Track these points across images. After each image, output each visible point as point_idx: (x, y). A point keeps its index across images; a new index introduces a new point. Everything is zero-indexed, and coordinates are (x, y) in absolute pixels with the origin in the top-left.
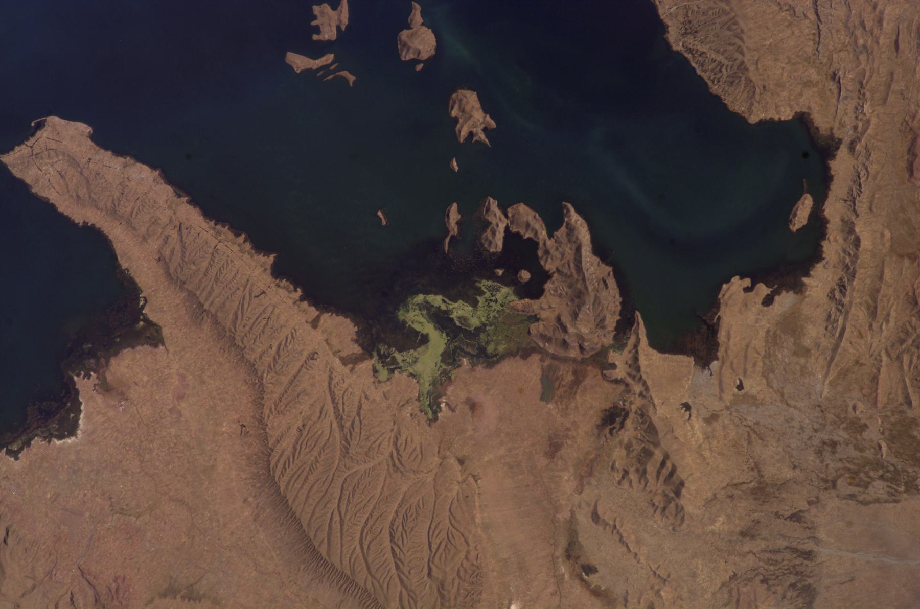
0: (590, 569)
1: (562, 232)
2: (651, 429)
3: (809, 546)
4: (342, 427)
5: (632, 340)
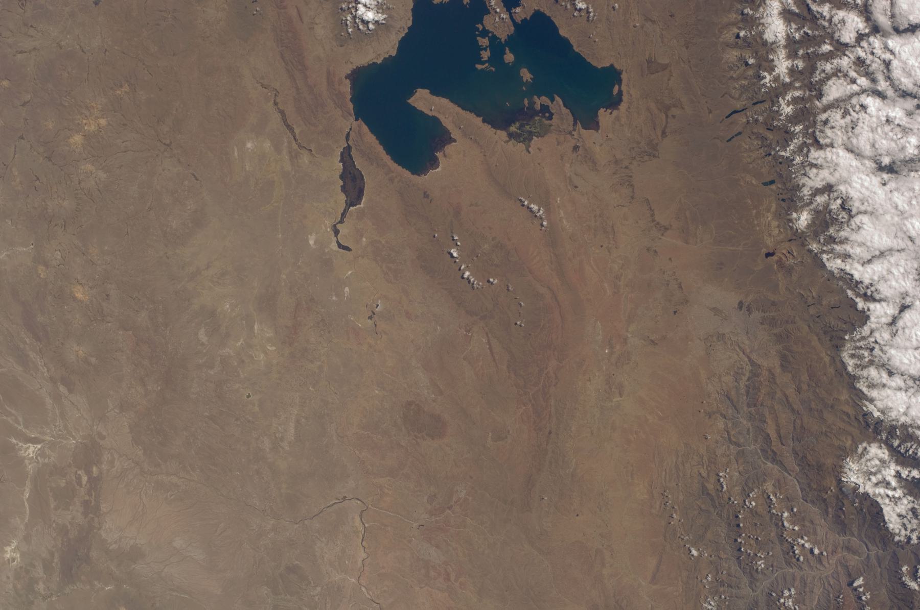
0: (576, 187)
1: (555, 102)
2: (586, 150)
3: (631, 174)
4: (507, 159)
5: (577, 128)
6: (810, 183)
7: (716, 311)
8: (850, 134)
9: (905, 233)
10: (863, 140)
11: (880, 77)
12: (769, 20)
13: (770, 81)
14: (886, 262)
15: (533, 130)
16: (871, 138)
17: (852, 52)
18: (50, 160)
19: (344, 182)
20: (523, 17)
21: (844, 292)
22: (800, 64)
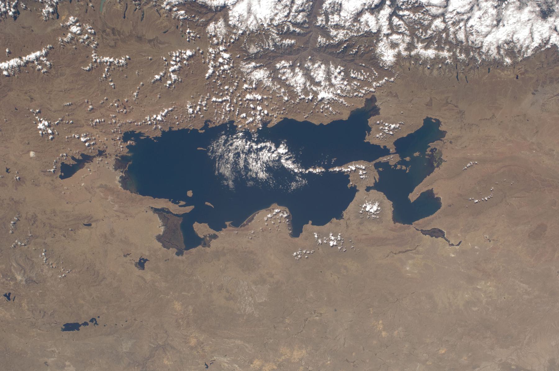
0: (466, 146)
6: (494, 54)
8: (480, 34)
9: (526, 22)
10: (484, 30)
11: (462, 17)
12: (426, 55)
13: (450, 60)
14: (535, 32)
15: (438, 157)
16: (484, 26)
17: (449, 26)
18: (388, 347)
19: (434, 236)
20: (394, 149)
21: (541, 52)
22: (447, 47)
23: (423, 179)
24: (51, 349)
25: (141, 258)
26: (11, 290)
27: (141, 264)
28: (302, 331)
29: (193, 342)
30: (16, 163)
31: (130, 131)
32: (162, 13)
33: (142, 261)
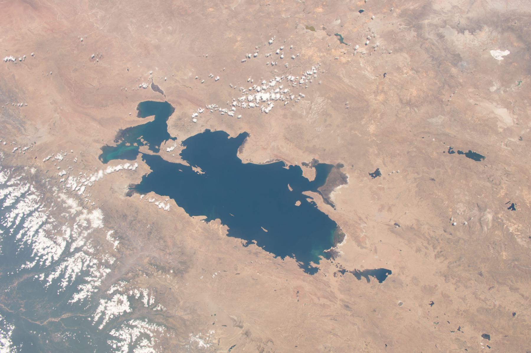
7: (40, 137)
23: (136, 126)
24: (507, 148)
25: (373, 178)
26: (504, 211)
27: (377, 173)
28: (293, 67)
29: (381, 98)
30: (420, 306)
31: (307, 273)
32: (217, 340)
33: (374, 175)
